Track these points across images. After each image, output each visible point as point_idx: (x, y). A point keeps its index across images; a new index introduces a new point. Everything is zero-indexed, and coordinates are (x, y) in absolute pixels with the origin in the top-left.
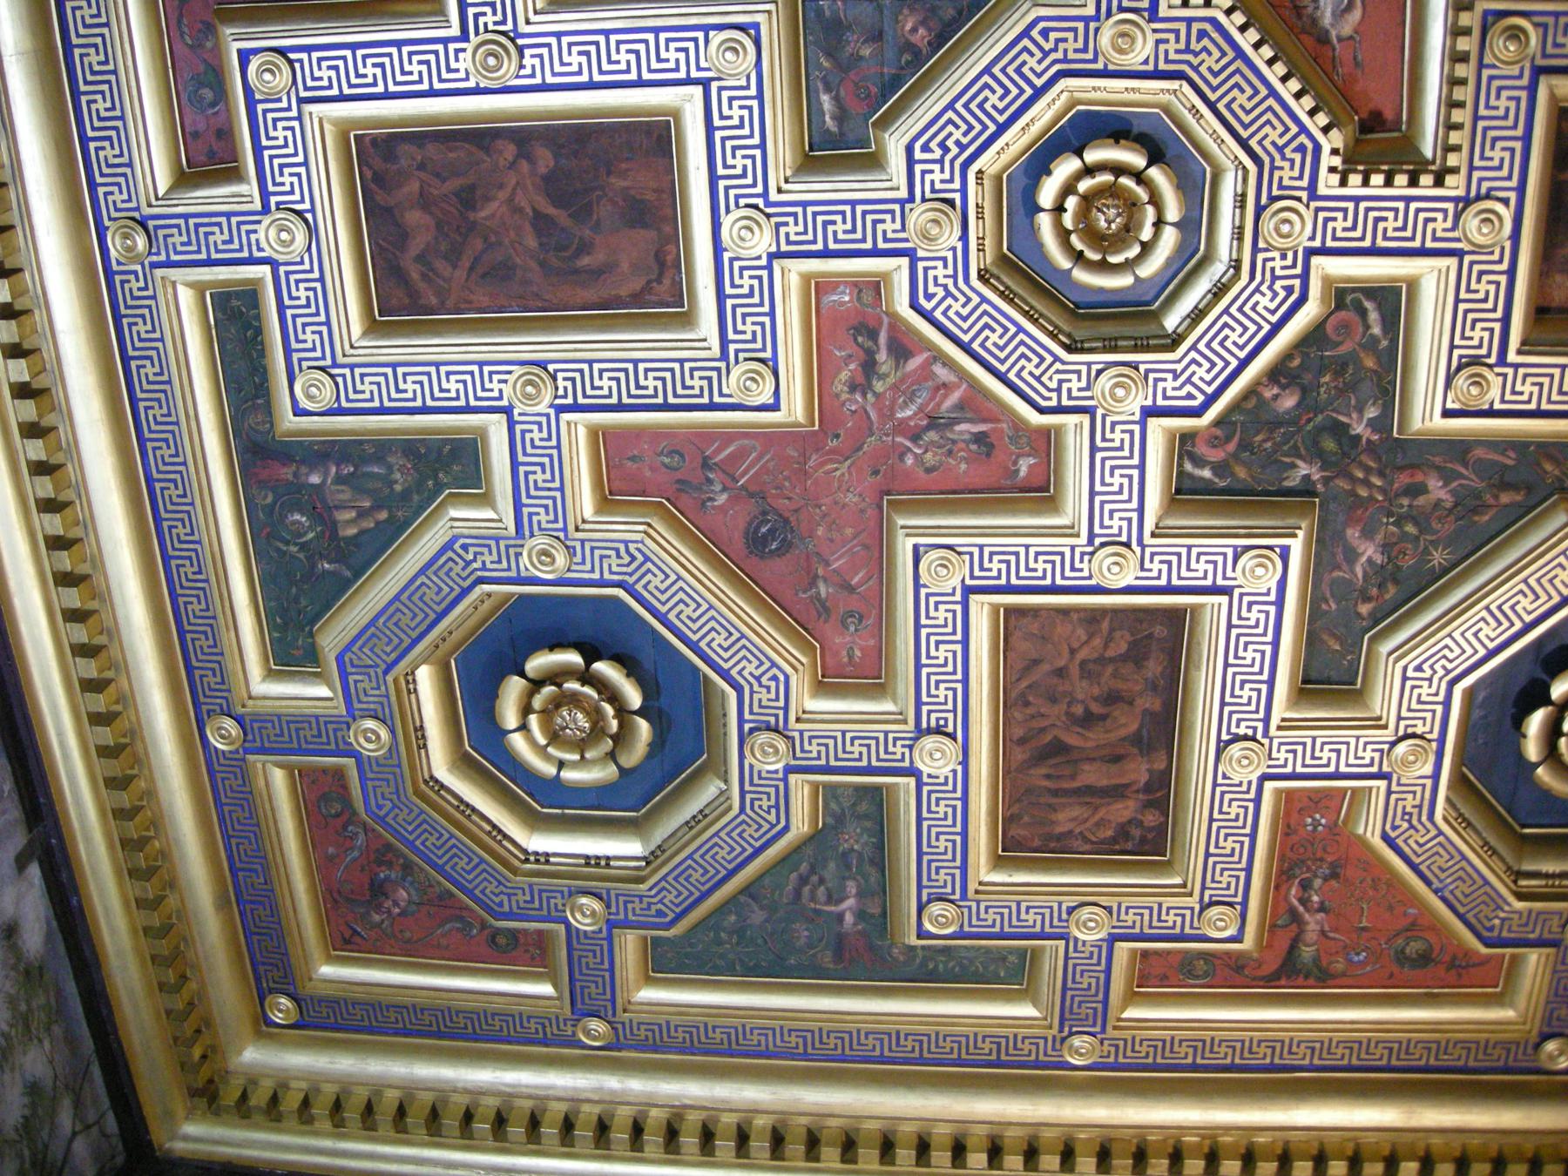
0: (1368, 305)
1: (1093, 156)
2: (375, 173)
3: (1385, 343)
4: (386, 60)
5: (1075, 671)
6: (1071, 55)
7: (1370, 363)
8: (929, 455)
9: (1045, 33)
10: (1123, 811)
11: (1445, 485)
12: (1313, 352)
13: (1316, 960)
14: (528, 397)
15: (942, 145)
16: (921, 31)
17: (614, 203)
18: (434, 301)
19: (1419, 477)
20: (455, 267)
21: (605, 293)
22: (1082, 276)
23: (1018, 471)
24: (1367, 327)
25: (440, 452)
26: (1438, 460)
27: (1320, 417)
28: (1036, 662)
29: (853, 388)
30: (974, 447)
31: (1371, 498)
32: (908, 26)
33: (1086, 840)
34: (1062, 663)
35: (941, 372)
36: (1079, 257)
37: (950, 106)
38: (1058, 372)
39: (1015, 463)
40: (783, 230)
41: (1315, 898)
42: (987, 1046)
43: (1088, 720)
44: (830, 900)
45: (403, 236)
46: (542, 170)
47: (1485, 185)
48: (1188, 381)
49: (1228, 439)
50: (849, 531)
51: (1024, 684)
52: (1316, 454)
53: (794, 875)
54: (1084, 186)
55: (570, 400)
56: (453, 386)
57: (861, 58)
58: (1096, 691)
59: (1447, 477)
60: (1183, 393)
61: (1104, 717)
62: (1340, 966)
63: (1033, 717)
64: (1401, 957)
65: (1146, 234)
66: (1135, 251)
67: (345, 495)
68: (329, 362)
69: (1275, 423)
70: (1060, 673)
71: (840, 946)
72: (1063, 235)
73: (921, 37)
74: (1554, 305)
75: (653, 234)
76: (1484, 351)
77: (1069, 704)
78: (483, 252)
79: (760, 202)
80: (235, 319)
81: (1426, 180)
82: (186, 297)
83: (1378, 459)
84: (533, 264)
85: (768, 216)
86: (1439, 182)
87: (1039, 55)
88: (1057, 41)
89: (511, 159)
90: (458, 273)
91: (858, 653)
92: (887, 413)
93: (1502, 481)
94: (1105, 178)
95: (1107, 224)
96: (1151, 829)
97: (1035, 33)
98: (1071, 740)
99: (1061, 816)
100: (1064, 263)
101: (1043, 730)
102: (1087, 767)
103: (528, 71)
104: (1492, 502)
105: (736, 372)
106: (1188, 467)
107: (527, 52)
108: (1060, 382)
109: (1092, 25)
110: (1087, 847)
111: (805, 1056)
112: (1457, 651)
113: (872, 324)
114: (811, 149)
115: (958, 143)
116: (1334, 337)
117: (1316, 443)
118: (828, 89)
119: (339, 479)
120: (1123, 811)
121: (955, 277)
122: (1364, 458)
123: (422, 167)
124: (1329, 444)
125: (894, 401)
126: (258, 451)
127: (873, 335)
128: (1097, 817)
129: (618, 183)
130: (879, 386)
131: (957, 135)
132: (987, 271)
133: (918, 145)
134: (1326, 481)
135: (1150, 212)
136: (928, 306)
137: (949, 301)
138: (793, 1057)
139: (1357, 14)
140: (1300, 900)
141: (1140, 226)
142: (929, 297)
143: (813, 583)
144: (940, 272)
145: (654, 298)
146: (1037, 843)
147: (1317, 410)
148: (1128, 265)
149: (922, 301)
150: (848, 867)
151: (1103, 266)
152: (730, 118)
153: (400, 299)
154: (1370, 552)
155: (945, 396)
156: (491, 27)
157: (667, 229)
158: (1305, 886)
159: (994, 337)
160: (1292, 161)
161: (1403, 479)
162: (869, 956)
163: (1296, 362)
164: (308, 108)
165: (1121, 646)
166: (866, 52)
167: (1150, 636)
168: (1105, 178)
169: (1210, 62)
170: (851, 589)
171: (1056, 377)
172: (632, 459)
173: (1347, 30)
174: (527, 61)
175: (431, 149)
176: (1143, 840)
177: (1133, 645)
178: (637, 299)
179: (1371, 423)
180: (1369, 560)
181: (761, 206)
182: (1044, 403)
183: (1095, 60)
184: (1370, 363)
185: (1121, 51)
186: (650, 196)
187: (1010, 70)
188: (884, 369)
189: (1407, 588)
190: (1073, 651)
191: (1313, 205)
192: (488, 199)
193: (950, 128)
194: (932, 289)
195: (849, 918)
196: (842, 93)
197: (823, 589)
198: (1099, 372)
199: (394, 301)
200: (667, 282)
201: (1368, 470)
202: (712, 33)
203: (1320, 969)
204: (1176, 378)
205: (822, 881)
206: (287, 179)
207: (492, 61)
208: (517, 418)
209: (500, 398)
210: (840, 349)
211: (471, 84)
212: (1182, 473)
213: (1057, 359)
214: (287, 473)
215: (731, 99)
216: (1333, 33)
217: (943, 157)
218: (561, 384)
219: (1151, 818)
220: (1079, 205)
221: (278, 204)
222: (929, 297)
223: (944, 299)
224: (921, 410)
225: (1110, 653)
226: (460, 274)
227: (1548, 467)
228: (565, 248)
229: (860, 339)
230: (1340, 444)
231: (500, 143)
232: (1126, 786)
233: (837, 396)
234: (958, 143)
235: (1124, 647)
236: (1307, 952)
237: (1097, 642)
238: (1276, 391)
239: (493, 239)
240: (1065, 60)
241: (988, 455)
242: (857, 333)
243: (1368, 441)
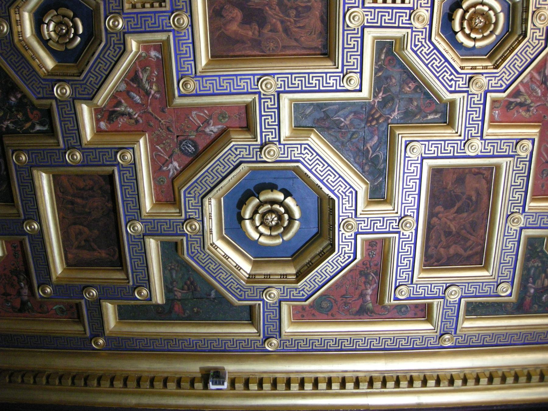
1: (457, 28)
2: (436, 262)
4: (403, 257)
6: (424, 37)
9: (416, 46)
14: (517, 222)
15: (450, 81)
16: (410, 85)
17: (456, 187)
18: (480, 247)
20: (470, 240)
21: (485, 192)
22: (498, 31)
25: (531, 250)
29: (528, 110)
32: (408, 89)
35: (525, 81)
36: (492, 33)
37: (437, 78)
38: (532, 40)
40: (473, 135)
45: (457, 255)
46: (442, 209)
54: (467, 31)
55: (521, 208)
56: (510, 245)
57: (417, 105)
65: (486, 8)
66: (491, 13)
67: (539, 282)
68: (495, 284)
72: (484, 38)
73: (412, 85)
75: (468, 176)
78: (466, 230)
79: (463, 142)
80: (476, 310)
82: (467, 324)
84: (472, 215)
85: (468, 140)
87: (423, 48)
88: (419, 41)
89: (437, 219)
90: (472, 239)
92: (539, 99)
94: (465, 24)
97: (415, 49)
100: (493, 37)
103: (412, 214)
105: (519, 152)
107: (406, 213)
108: (536, 39)
109: (414, 29)
113: (507, 103)
114: (446, 123)
115: (450, 76)
118: (427, 116)
119: (534, 283)
121: (495, 77)
123: (436, 247)
125: (535, 96)
126: (519, 308)
127: (511, 103)
129: (450, 186)
130: (529, 101)
131: (447, 75)
132: (494, 65)
133: (450, 89)
135: (479, 7)
136: (504, 86)
137: (503, 79)
141: (483, 11)
142: (501, 86)
144: (493, 82)
145: (489, 176)
148: (496, 14)
149: (502, 88)
151: (496, 24)
152: (434, 151)
153: (478, 258)
155: (535, 78)
156: (397, 224)
157: (467, 171)
159: (518, 63)
164: (414, 281)
166: (415, 103)
168: (465, 24)
171: (534, 41)
172: (542, 187)
174: (409, 214)
175: (431, 243)
178: (489, 182)
181: (464, 142)
182: (543, 45)
183: (426, 28)
185: (424, 20)
186: (455, 176)
187: (427, 58)
188: (523, 100)
192: (449, 227)
193: (445, 78)
194: (499, 85)
196: (428, 112)
198: (534, 25)
199: (478, 260)
200: (484, 172)
202: (407, 155)
206: (435, 290)
207: (408, 225)
208: (524, 226)
209: (517, 230)
210: (514, 115)
211: (414, 232)
213: (528, 41)
214: (528, 299)
215: (429, 150)
217: (454, 81)
218: (515, 210)
220: (474, 33)
221: (442, 294)
222: (501, 86)
223: (503, 81)
224: (539, 87)
226: (472, 238)
228: (469, 204)
229: (511, 108)
231: (432, 222)
233: (530, 116)
234: (450, 76)
239: (462, 227)
240: (425, 39)
242: (509, 110)
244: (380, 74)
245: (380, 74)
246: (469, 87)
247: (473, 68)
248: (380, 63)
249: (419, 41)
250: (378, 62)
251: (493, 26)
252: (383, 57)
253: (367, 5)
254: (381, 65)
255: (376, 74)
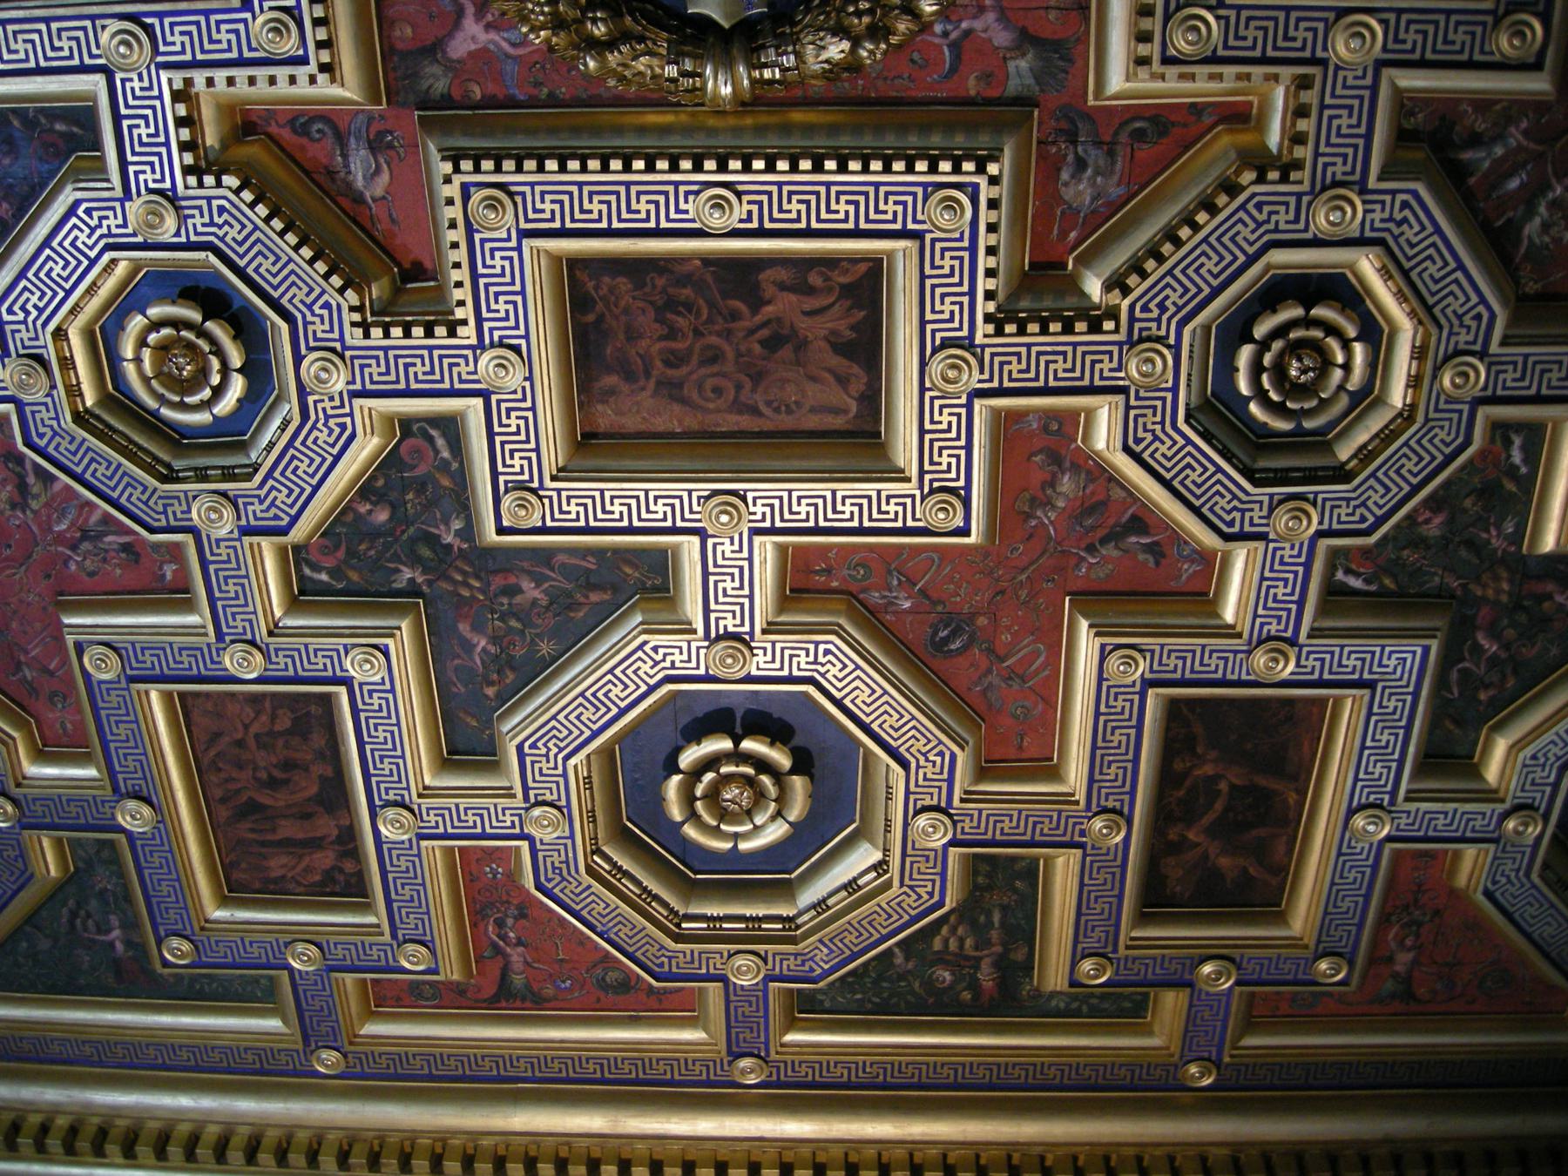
0: (434, 433)
3: (455, 465)
5: (251, 742)
7: (446, 482)
8: (88, 562)
10: (325, 859)
11: (537, 586)
12: (393, 474)
13: (528, 986)
15: (23, 308)
19: (512, 580)
22: (166, 412)
23: (164, 575)
24: (437, 452)
26: (525, 565)
27: (412, 530)
28: (217, 735)
29: (14, 506)
30: (123, 555)
31: (473, 597)
33: (299, 883)
34: (239, 736)
39: (161, 568)
41: (512, 935)
42: (250, 1058)
43: (273, 784)
44: (99, 931)
47: (496, 334)
48: (273, 504)
49: (337, 547)
50: (38, 625)
51: (212, 753)
52: (415, 561)
53: (65, 911)
58: (274, 760)
59: (539, 580)
60: (270, 514)
61: (287, 782)
62: (549, 991)
63: (227, 781)
64: (603, 985)
66: (207, 393)
69: (375, 534)
70: (240, 744)
71: (117, 966)
72: (146, 380)
74: (601, 430)
76: (526, 477)
77: (255, 770)
81: (440, 331)
83: (471, 564)
86: (452, 333)
91: (69, 726)
93: (588, 583)
95: (183, 368)
96: (352, 875)
98: (265, 800)
99: (272, 863)
101: (238, 791)
102: (283, 822)
104: (582, 600)
106: (307, 571)
108: (165, 506)
110: (302, 889)
111: (101, 1064)
112: (566, 732)
116: (407, 459)
117: (413, 551)
120: (325, 859)
122: (459, 563)
124: (426, 552)
125: (49, 517)
128: (303, 865)
130: (34, 505)
131: (34, 299)
134: (430, 583)
136: (42, 443)
138: (92, 1064)
139: (385, 177)
140: (499, 936)
142: (41, 436)
143: (18, 666)
144: (45, 415)
146: (257, 885)
147: (409, 523)
148: (207, 405)
150: (108, 904)
151: (183, 407)
154: (483, 643)
158: (500, 924)
160: (322, 317)
161: (498, 582)
162: (136, 980)
163: (381, 483)
165: (284, 723)
167: (308, 714)
169: (233, 233)
170: (52, 674)
171: (161, 502)
173: (379, 192)
176: (348, 884)
177: (295, 721)
179: (458, 533)
180: (484, 649)
182: (156, 524)
184: (446, 482)
188: (35, 490)
189: (524, 673)
190: (246, 727)
191: (348, 354)
195: (119, 946)
197: (28, 674)
198: (195, 497)
201: (464, 573)
203: (533, 994)
204: (261, 502)
205: (89, 916)
212: (302, 578)
216: (368, 194)
219: (349, 866)
222: (41, 436)
224: (73, 524)
225: (278, 728)
227: (628, 570)
230: (435, 552)
232: (322, 838)
234: (35, 306)
235: (287, 723)
236: (518, 980)
237: (264, 718)
238: (368, 507)
240: (110, 235)
241: (137, 562)
243: (460, 549)
244: (16, 123)
245: (16, 123)
246: (19, 356)
247: (67, 363)
248: (43, 121)
249: (101, 218)
250: (46, 116)
251: (177, 399)
252: (59, 127)
253: (164, 76)
254: (38, 123)
255: (14, 111)
